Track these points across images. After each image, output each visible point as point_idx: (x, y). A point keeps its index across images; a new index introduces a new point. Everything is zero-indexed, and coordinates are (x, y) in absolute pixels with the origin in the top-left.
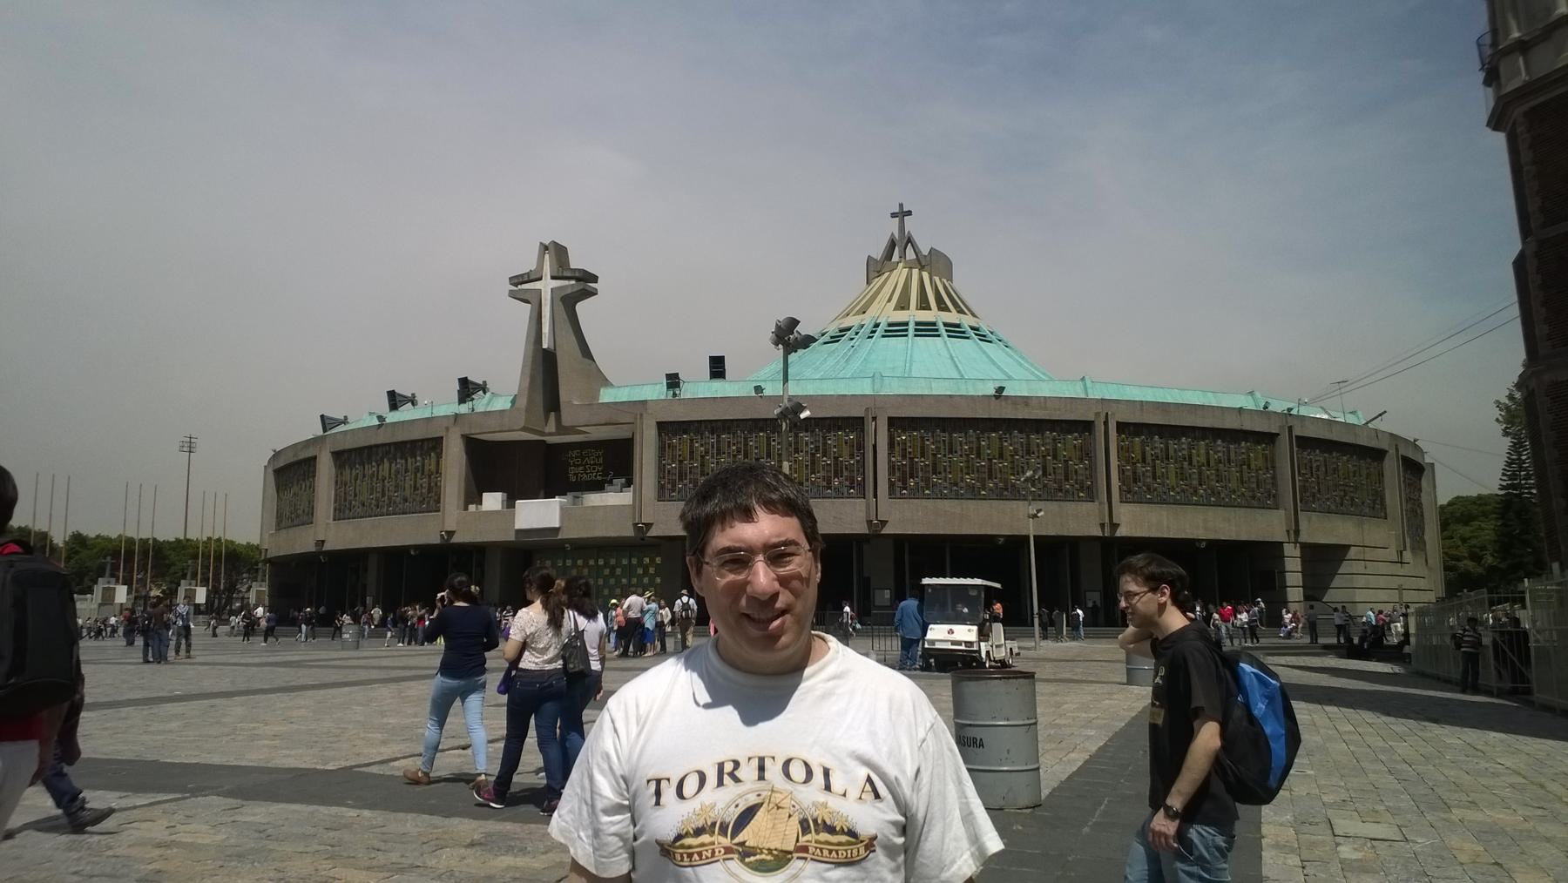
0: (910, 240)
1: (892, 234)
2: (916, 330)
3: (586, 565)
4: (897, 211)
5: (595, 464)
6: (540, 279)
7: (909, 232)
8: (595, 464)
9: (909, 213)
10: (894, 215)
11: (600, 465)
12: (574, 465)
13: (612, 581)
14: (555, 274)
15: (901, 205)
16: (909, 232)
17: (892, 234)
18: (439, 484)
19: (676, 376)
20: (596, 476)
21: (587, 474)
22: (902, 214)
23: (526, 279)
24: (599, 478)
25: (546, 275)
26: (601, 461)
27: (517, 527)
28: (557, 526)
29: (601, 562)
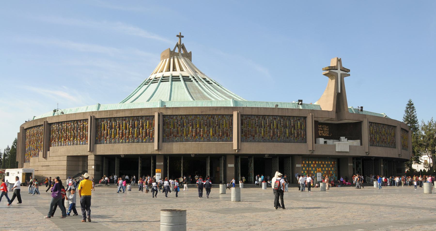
0: (183, 47)
1: (178, 42)
2: (180, 79)
3: (315, 163)
4: (179, 34)
5: (326, 131)
6: (337, 69)
7: (183, 43)
8: (326, 131)
9: (183, 37)
10: (178, 36)
11: (328, 131)
12: (320, 130)
13: (323, 169)
14: (342, 69)
15: (180, 33)
16: (183, 43)
17: (178, 42)
18: (380, 138)
19: (363, 107)
20: (327, 135)
21: (324, 133)
22: (180, 36)
23: (334, 68)
24: (328, 135)
25: (339, 69)
26: (328, 130)
27: (337, 151)
28: (349, 151)
29: (320, 162)
